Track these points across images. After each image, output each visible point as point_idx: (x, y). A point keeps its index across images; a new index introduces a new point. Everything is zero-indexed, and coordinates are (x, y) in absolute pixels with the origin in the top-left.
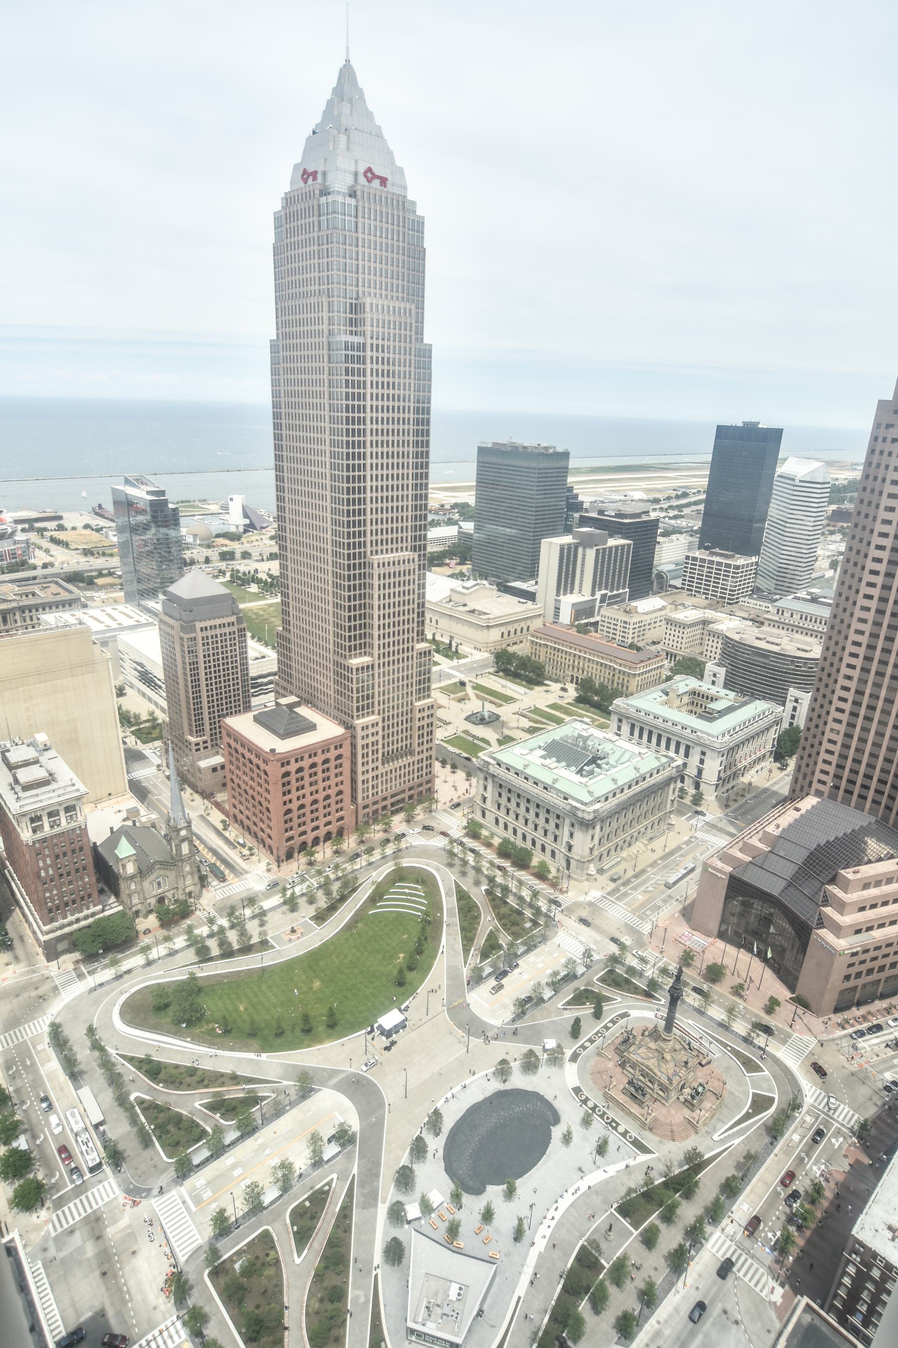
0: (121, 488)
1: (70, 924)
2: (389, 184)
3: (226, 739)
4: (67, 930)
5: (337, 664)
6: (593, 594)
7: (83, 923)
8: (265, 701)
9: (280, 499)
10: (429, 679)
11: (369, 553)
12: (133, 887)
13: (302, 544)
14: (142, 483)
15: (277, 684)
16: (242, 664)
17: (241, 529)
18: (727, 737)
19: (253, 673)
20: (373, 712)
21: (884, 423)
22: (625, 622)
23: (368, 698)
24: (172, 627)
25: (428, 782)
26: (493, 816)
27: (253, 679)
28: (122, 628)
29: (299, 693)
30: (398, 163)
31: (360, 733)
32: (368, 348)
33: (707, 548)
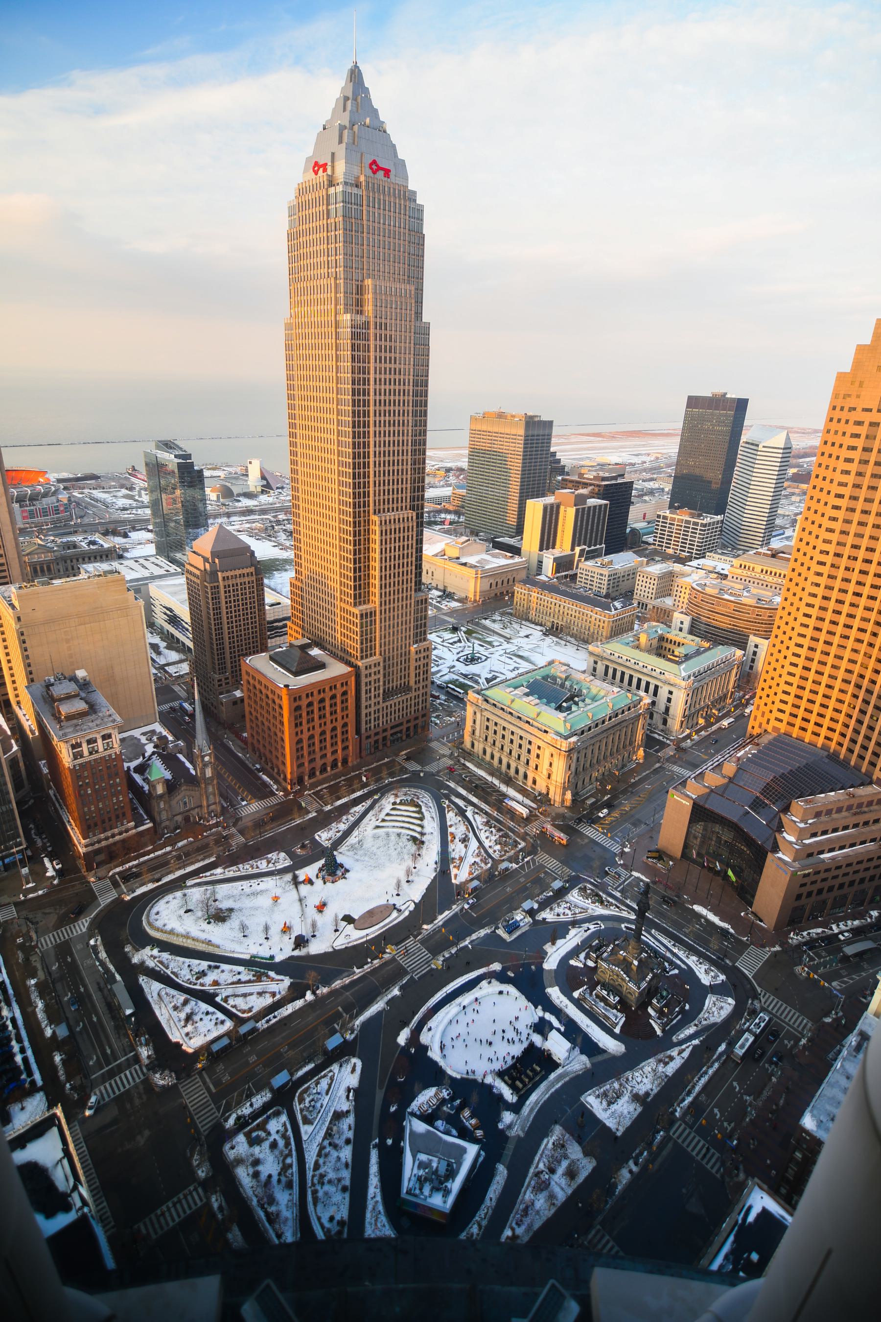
0: (154, 451)
1: (107, 839)
2: (392, 174)
3: (245, 677)
4: (104, 843)
6: (573, 549)
7: (117, 838)
8: (279, 644)
10: (425, 623)
11: (371, 511)
12: (162, 805)
14: (171, 448)
17: (259, 489)
18: (692, 678)
19: (270, 617)
21: (842, 393)
22: (602, 575)
25: (424, 716)
26: (481, 746)
28: (153, 578)
29: (310, 636)
30: (401, 156)
31: (364, 672)
32: (372, 326)
33: (678, 508)
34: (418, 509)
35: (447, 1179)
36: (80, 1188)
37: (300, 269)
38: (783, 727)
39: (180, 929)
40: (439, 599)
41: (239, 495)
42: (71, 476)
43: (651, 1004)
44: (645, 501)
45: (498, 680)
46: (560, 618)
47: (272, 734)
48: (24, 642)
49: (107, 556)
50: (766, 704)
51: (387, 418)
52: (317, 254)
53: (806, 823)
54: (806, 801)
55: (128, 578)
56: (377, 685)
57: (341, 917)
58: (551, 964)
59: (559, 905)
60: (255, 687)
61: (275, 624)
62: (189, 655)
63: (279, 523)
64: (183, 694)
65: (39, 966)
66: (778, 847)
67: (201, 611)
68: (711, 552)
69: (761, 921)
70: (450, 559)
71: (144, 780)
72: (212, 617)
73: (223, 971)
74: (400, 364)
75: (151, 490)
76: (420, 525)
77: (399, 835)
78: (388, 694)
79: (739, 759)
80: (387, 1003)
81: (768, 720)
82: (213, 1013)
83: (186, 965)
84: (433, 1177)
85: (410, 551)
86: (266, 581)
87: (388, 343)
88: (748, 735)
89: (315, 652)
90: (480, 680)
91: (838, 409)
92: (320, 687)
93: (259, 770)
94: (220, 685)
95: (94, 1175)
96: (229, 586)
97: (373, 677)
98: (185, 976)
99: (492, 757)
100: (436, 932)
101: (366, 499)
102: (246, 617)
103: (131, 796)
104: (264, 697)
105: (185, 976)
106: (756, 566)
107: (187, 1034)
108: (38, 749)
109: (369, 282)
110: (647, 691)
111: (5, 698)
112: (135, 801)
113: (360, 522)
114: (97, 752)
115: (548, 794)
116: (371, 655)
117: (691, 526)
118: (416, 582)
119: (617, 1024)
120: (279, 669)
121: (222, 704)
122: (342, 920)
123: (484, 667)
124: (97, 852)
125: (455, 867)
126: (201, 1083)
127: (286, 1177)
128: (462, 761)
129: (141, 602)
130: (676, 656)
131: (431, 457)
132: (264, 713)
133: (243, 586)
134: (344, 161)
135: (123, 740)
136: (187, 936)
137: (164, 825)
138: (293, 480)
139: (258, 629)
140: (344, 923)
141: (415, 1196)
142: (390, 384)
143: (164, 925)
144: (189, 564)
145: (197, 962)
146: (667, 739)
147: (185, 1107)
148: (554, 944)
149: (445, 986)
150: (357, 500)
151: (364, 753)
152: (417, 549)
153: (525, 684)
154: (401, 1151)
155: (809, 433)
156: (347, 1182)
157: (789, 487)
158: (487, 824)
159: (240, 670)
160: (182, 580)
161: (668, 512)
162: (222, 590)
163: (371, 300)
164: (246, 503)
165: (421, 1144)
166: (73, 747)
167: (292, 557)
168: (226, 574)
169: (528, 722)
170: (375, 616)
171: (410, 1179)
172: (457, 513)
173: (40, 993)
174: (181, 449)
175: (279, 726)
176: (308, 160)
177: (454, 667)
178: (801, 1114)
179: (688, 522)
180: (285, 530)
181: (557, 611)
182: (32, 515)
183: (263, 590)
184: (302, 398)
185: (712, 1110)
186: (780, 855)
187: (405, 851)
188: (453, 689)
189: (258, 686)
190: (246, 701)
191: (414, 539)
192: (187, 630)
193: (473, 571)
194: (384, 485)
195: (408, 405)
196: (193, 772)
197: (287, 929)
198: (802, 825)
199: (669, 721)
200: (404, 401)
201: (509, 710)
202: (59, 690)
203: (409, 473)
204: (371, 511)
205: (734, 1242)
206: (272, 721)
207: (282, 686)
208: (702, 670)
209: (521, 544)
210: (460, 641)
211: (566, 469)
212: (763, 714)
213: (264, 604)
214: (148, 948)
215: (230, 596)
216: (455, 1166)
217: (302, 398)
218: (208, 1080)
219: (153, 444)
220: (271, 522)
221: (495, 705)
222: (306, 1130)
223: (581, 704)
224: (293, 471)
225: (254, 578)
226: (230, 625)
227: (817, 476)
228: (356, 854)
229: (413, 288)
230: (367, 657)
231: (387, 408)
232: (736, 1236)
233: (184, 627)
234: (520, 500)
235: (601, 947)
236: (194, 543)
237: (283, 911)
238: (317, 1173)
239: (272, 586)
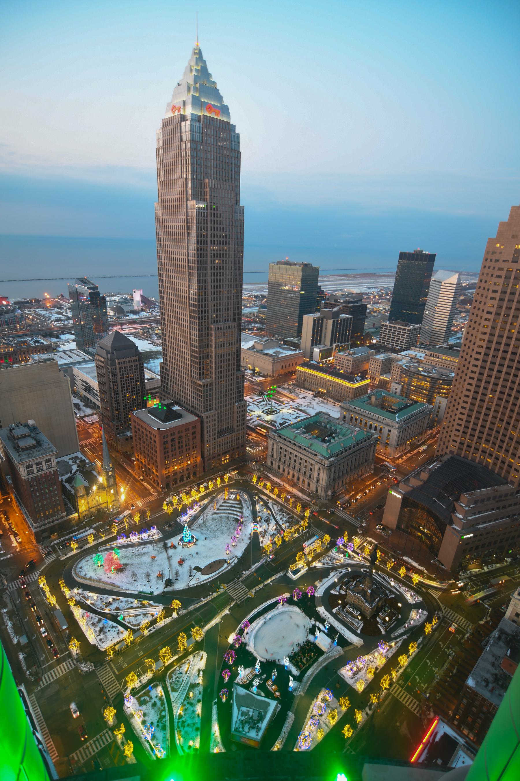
1: (49, 523)
4: (47, 526)
5: (192, 382)
6: (331, 345)
7: (56, 522)
13: (174, 317)
15: (161, 394)
20: (212, 409)
23: (210, 401)
26: (277, 464)
27: (147, 390)
29: (172, 398)
31: (205, 420)
33: (393, 320)
35: (258, 722)
36: (36, 733)
38: (455, 450)
39: (95, 577)
41: (128, 312)
42: (23, 300)
43: (378, 615)
45: (287, 424)
50: (446, 437)
53: (469, 507)
54: (469, 494)
55: (60, 363)
56: (214, 428)
57: (193, 567)
58: (319, 594)
59: (324, 558)
62: (98, 410)
63: (153, 329)
65: (8, 601)
66: (453, 521)
68: (413, 346)
69: (443, 565)
70: (258, 351)
71: (71, 487)
73: (122, 602)
75: (72, 308)
76: (239, 330)
77: (228, 518)
78: (220, 433)
79: (430, 469)
80: (222, 618)
81: (447, 447)
82: (116, 627)
83: (99, 598)
84: (250, 720)
86: (145, 365)
88: (435, 456)
89: (176, 408)
90: (276, 425)
91: (489, 260)
93: (142, 480)
95: (45, 726)
96: (122, 368)
97: (211, 423)
98: (99, 605)
99: (284, 470)
100: (250, 575)
102: (133, 384)
103: (63, 497)
104: (144, 436)
105: (99, 605)
107: (101, 640)
112: (66, 500)
113: (202, 329)
114: (42, 470)
115: (317, 492)
116: (210, 410)
117: (402, 331)
118: (237, 365)
119: (358, 628)
120: (154, 418)
121: (119, 440)
122: (194, 569)
123: (278, 417)
124: (43, 531)
125: (262, 536)
126: (109, 669)
127: (162, 723)
128: (266, 473)
129: (68, 378)
130: (393, 409)
131: (246, 290)
132: (145, 445)
133: (131, 368)
134: (191, 105)
135: (58, 463)
136: (100, 581)
138: (161, 303)
140: (195, 571)
141: (240, 732)
143: (86, 575)
144: (99, 355)
145: (106, 596)
146: (388, 458)
147: (100, 684)
148: (321, 581)
149: (256, 607)
151: (206, 470)
153: (303, 426)
154: (231, 706)
155: (471, 275)
156: (199, 725)
157: (459, 307)
158: (281, 510)
160: (93, 365)
161: (388, 322)
165: (243, 701)
166: (28, 467)
167: (161, 350)
168: (120, 361)
169: (305, 449)
171: (236, 722)
173: (9, 617)
174: (91, 283)
175: (154, 453)
176: (168, 105)
177: (260, 416)
178: (467, 677)
179: (400, 329)
181: (322, 382)
183: (143, 370)
185: (414, 677)
186: (454, 526)
187: (232, 527)
188: (260, 430)
189: (141, 429)
190: (134, 438)
192: (97, 395)
197: (160, 576)
198: (467, 509)
201: (294, 442)
202: (19, 432)
203: (232, 298)
204: (210, 322)
205: (427, 753)
206: (150, 450)
207: (156, 429)
208: (408, 418)
209: (300, 342)
210: (263, 401)
212: (444, 443)
216: (263, 713)
218: (113, 667)
220: (148, 328)
221: (285, 439)
222: (173, 696)
223: (336, 438)
224: (161, 297)
226: (124, 392)
227: (476, 301)
228: (202, 529)
230: (207, 410)
232: (428, 750)
233: (94, 393)
234: (299, 315)
235: (349, 582)
237: (158, 565)
238: (181, 720)
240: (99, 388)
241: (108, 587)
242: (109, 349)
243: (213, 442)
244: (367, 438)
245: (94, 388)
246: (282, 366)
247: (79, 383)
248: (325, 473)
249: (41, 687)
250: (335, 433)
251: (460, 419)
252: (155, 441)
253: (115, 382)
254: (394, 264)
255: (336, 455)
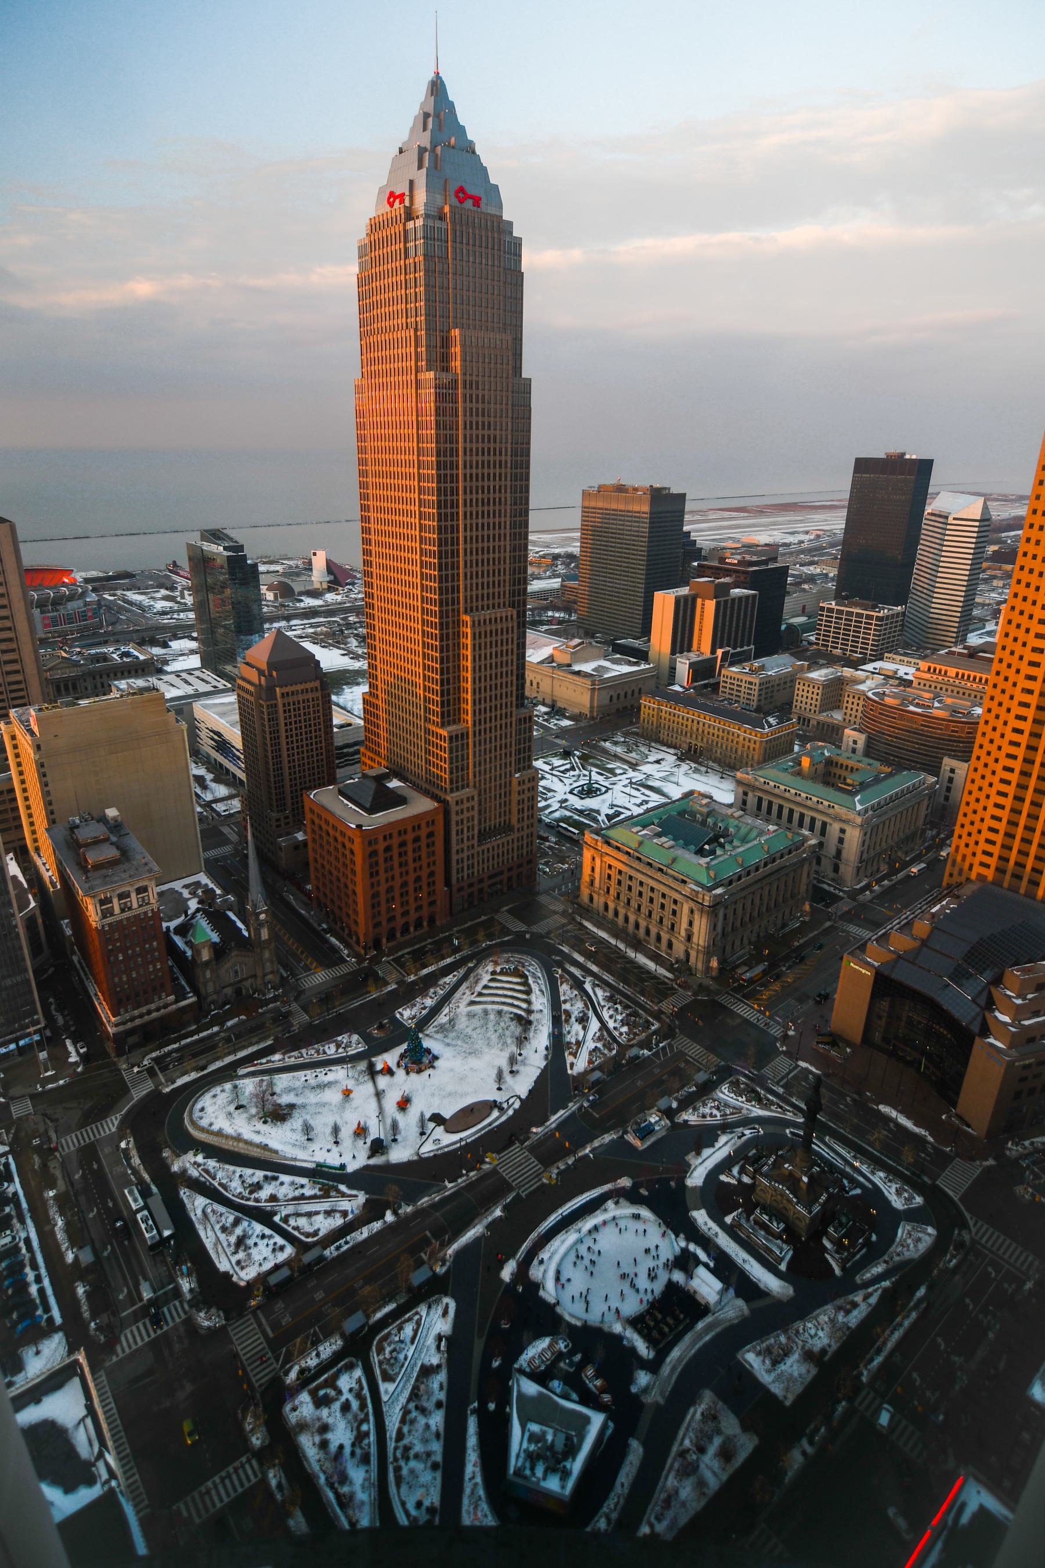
1: (141, 1016)
2: (483, 203)
3: (308, 815)
4: (138, 1022)
7: (154, 1015)
9: (366, 552)
10: (530, 747)
12: (208, 974)
14: (219, 538)
16: (326, 733)
17: (325, 586)
19: (338, 742)
20: (468, 786)
23: (463, 770)
24: (251, 694)
25: (529, 862)
26: (602, 900)
31: (454, 808)
33: (846, 598)
34: (519, 606)
35: (565, 1458)
36: (107, 1455)
37: (374, 320)
38: (990, 874)
39: (229, 1130)
40: (546, 717)
41: (301, 594)
42: (101, 575)
43: (826, 1233)
44: (804, 590)
45: (622, 817)
46: (700, 738)
47: (342, 886)
48: (44, 775)
49: (143, 670)
50: (967, 845)
51: (480, 496)
52: (392, 287)
53: (1024, 999)
54: (1025, 971)
55: (168, 696)
56: (470, 824)
57: (428, 1116)
58: (696, 1178)
59: (705, 1105)
60: (321, 828)
61: (345, 750)
62: (241, 788)
63: (349, 626)
64: (234, 837)
65: (58, 1173)
66: (989, 1030)
67: (255, 735)
68: (890, 652)
69: (969, 1126)
70: (560, 666)
71: (186, 943)
72: (268, 741)
73: (282, 1184)
74: (495, 429)
75: (194, 590)
76: (522, 625)
77: (500, 1013)
78: (484, 836)
79: (933, 915)
80: (488, 1227)
82: (270, 1237)
83: (237, 1175)
84: (548, 1453)
85: (510, 657)
86: (334, 698)
87: (480, 406)
88: (944, 884)
89: (394, 784)
90: (600, 818)
92: (400, 828)
93: (326, 931)
94: (278, 826)
95: (124, 1440)
96: (289, 704)
97: (466, 815)
98: (236, 1189)
99: (616, 914)
100: (549, 1136)
101: (456, 595)
103: (170, 963)
104: (331, 840)
105: (236, 1189)
106: (949, 669)
107: (238, 1262)
108: (59, 905)
109: (456, 333)
110: (812, 829)
111: (21, 843)
112: (175, 970)
113: (447, 623)
115: (688, 960)
116: (463, 787)
119: (782, 1259)
120: (351, 805)
121: (281, 849)
122: (431, 1119)
123: (604, 801)
124: (130, 1033)
125: (570, 1054)
126: (255, 1325)
127: (362, 1448)
128: (578, 918)
129: (184, 726)
130: (849, 785)
131: (535, 543)
132: (332, 859)
133: (306, 704)
135: (161, 894)
136: (238, 1138)
137: (210, 999)
138: (367, 574)
139: (324, 757)
140: (431, 1125)
141: (525, 1477)
142: (483, 454)
143: (211, 1125)
144: (244, 679)
145: (249, 1171)
146: (840, 890)
147: (236, 1356)
148: (699, 1154)
149: (560, 1206)
150: (444, 597)
152: (518, 654)
153: (656, 821)
154: (507, 1420)
155: (1011, 500)
156: (438, 1458)
157: (989, 568)
158: (610, 999)
159: (303, 807)
160: (232, 698)
161: (833, 603)
162: (281, 709)
163: (459, 354)
164: (310, 602)
165: (532, 1410)
166: (102, 902)
167: (366, 667)
169: (661, 870)
170: (468, 738)
171: (518, 1456)
172: (568, 610)
173: (59, 1207)
174: (231, 539)
175: (350, 876)
176: (381, 190)
177: (566, 800)
178: (1028, 1383)
180: (356, 635)
181: (695, 729)
182: (55, 622)
183: (330, 708)
184: (376, 475)
187: (508, 1033)
189: (324, 827)
190: (310, 845)
191: (515, 642)
192: (239, 758)
193: (588, 682)
194: (477, 577)
195: (506, 480)
196: (246, 934)
197: (361, 1131)
198: (1019, 1002)
199: (842, 867)
200: (500, 474)
201: (636, 854)
202: (85, 834)
203: (508, 562)
206: (342, 869)
207: (354, 826)
208: (882, 803)
209: (649, 647)
210: (573, 769)
211: (703, 553)
213: (331, 726)
214: (191, 1153)
215: (290, 717)
216: (575, 1440)
217: (376, 475)
218: (264, 1321)
219: (199, 533)
220: (339, 625)
221: (618, 848)
222: (386, 1388)
223: (728, 847)
224: (367, 563)
225: (319, 694)
226: (291, 752)
227: (1025, 554)
228: (446, 1036)
229: (510, 338)
230: (457, 789)
231: (480, 484)
232: (946, 1543)
233: (234, 755)
235: (760, 1158)
236: (248, 652)
237: (356, 1108)
238: (401, 1444)
239: (341, 704)
240: (244, 744)
241: (256, 1153)
242: (264, 667)
243: (470, 853)
244: (793, 847)
245: (234, 744)
246: (611, 697)
247: (204, 734)
248: (704, 921)
249: (117, 1356)
250: (725, 834)
251: (997, 805)
252: (352, 852)
253: (273, 718)
254: (842, 485)
255: (727, 881)
